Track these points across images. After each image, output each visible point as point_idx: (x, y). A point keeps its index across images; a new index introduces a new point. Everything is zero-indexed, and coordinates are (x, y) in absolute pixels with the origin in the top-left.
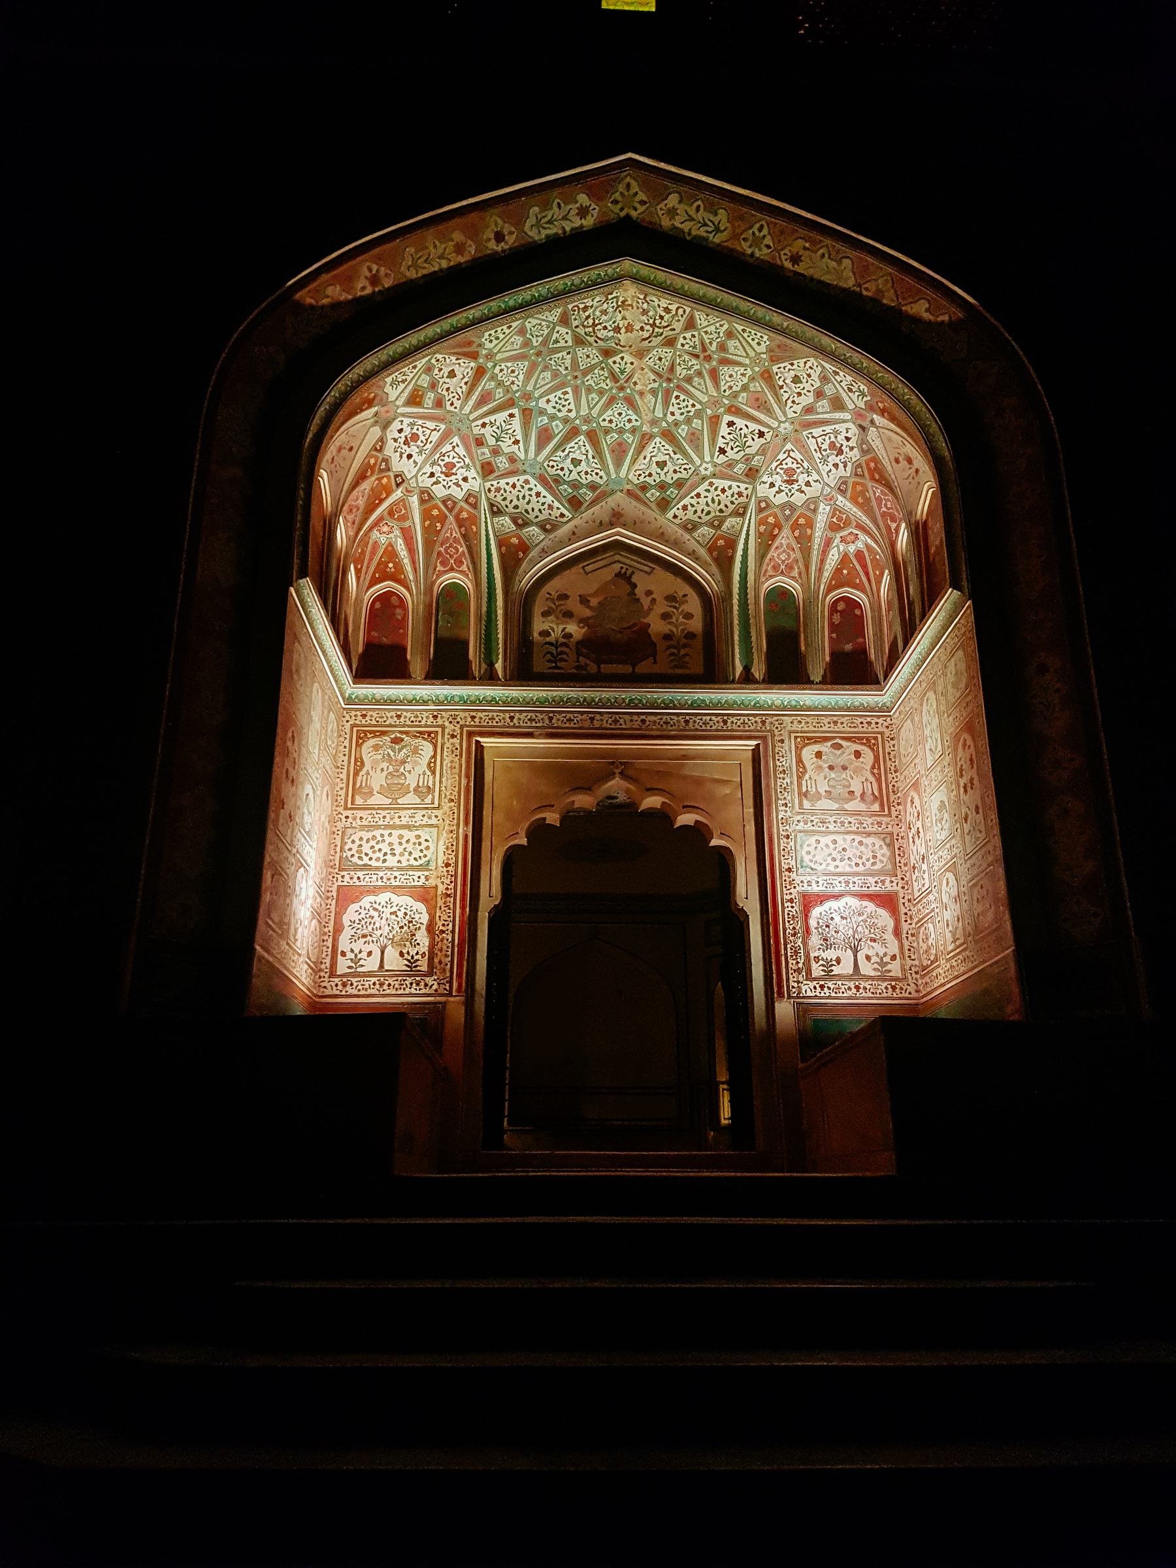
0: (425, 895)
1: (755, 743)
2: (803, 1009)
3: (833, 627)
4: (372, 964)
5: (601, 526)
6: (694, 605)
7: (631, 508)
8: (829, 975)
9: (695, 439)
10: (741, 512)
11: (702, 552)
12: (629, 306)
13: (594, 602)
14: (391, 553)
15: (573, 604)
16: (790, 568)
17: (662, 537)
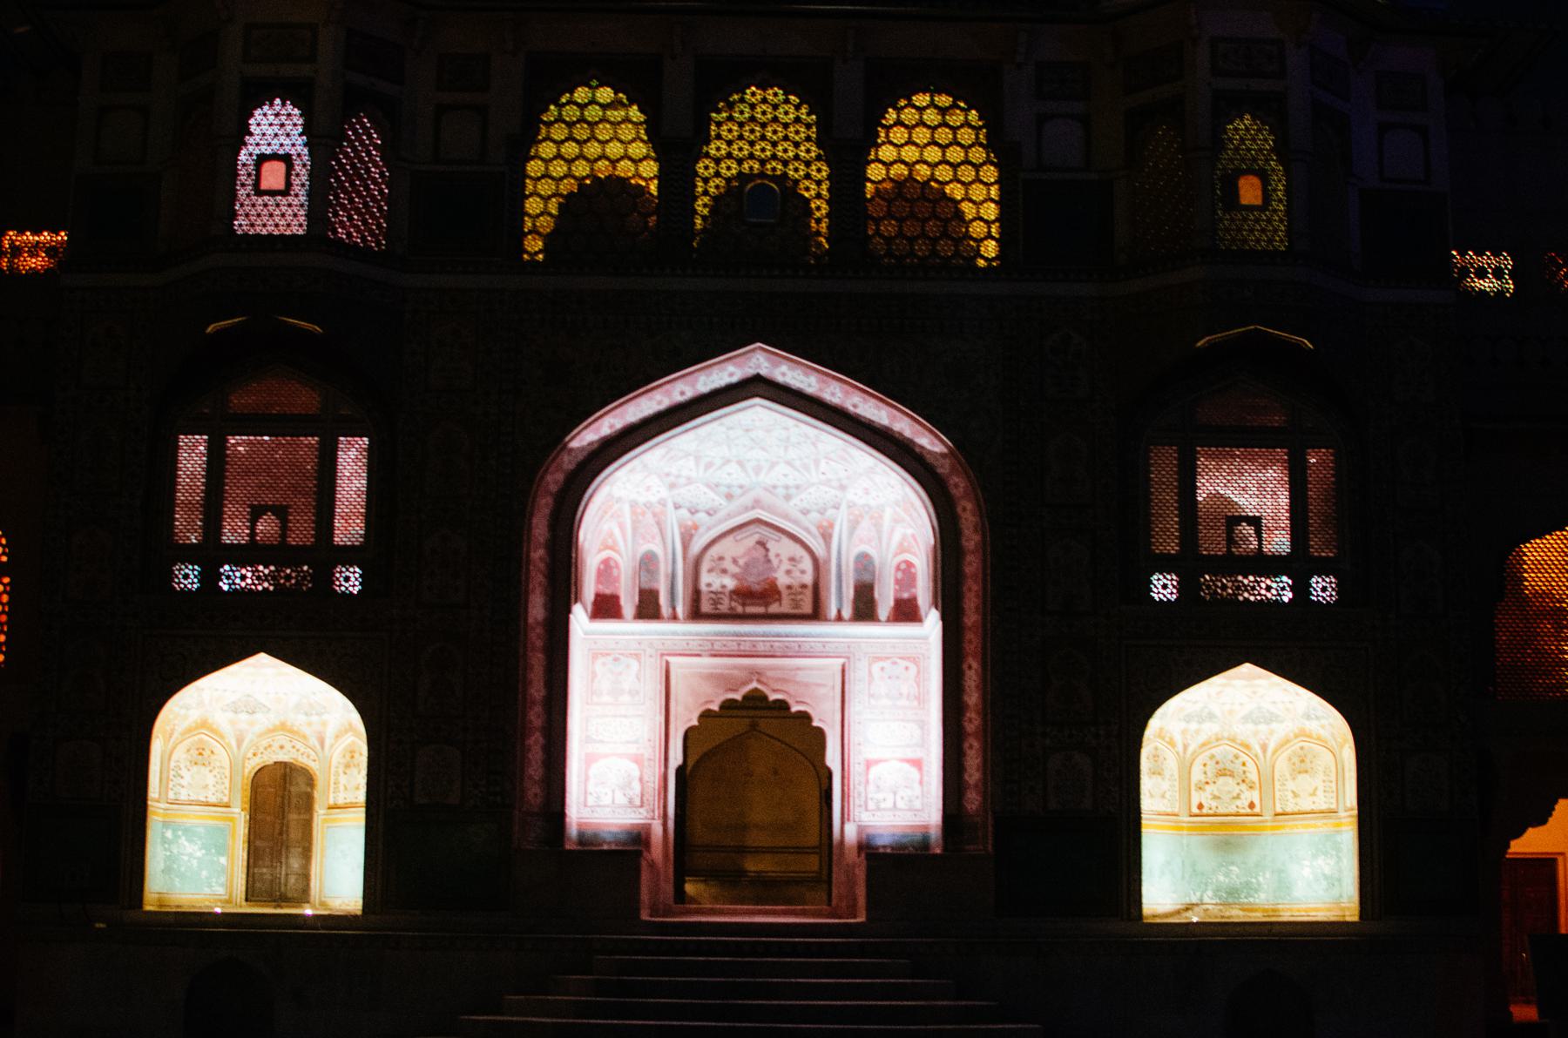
0: (637, 760)
1: (842, 661)
2: (861, 829)
3: (897, 582)
4: (607, 800)
5: (747, 509)
6: (807, 564)
7: (767, 498)
8: (879, 809)
9: (807, 468)
10: (837, 507)
11: (814, 530)
12: (758, 414)
13: (741, 562)
14: (611, 535)
15: (728, 564)
16: (870, 541)
17: (786, 517)
